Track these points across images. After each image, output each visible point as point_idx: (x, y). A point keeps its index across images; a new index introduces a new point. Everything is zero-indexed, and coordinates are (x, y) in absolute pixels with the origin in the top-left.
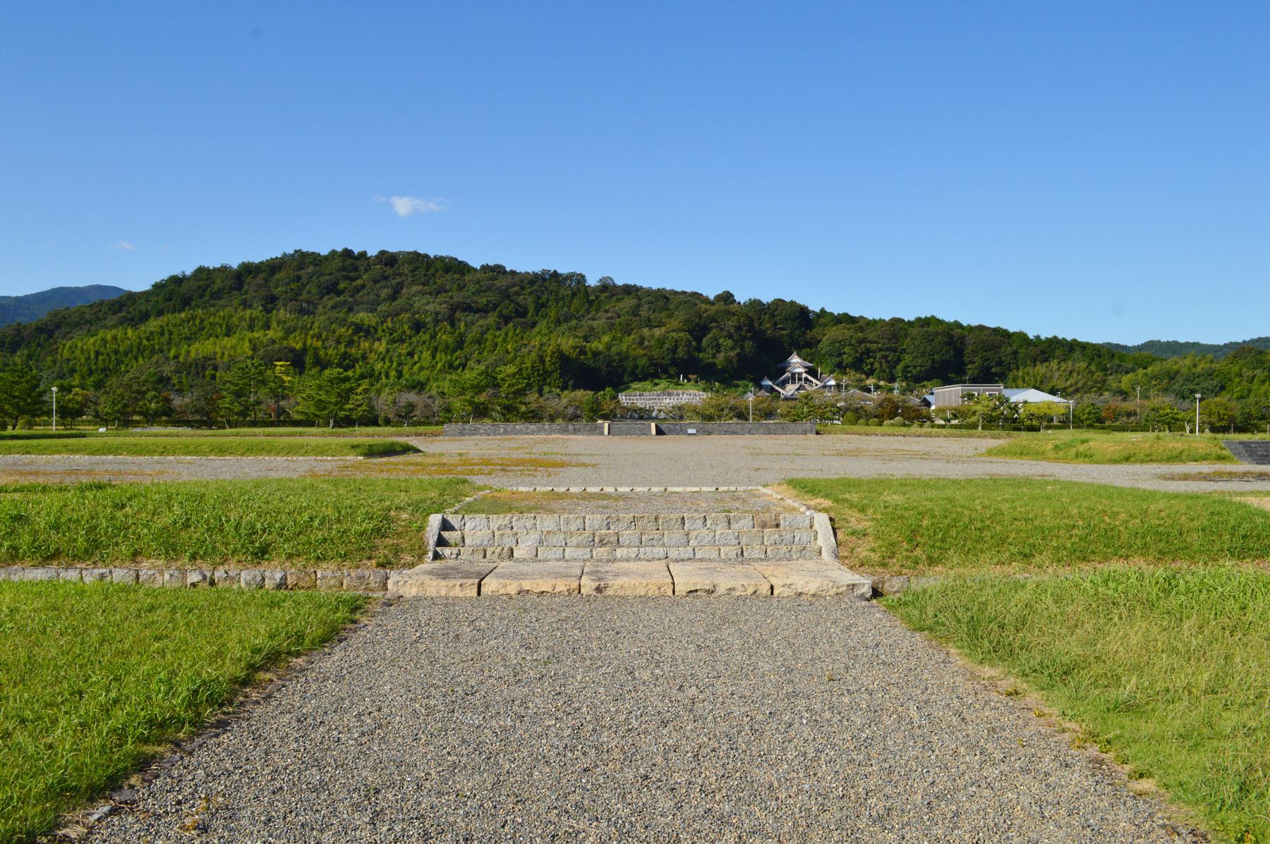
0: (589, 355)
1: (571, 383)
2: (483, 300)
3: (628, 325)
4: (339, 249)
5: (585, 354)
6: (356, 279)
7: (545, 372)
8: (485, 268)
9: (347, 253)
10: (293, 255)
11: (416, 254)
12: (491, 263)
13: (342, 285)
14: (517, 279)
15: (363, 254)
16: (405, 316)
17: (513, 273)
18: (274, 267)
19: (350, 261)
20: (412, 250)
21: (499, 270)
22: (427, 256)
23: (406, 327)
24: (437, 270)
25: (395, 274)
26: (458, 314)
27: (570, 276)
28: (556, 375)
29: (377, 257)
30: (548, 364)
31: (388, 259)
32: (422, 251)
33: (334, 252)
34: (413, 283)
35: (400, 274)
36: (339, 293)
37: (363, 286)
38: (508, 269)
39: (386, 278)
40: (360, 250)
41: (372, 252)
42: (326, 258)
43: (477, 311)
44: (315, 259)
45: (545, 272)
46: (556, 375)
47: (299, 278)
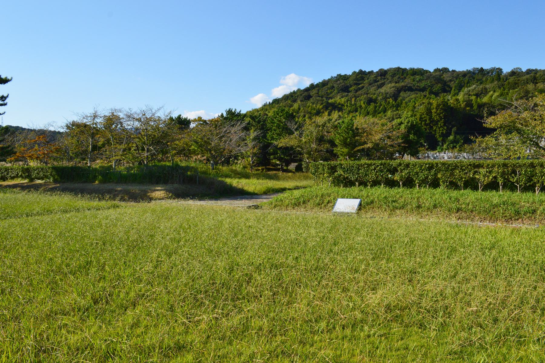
0: (475, 107)
1: (454, 129)
2: (422, 85)
3: (516, 84)
4: (357, 71)
5: (471, 106)
6: (359, 84)
7: (432, 120)
8: (436, 70)
9: (361, 72)
10: (336, 77)
11: (399, 69)
12: (440, 67)
13: (351, 89)
14: (455, 75)
15: (371, 72)
16: (362, 97)
17: (454, 71)
18: (324, 84)
19: (361, 75)
20: (397, 67)
21: (445, 70)
22: (405, 69)
23: (362, 102)
24: (407, 75)
25: (381, 79)
26: (402, 94)
27: (493, 70)
28: (441, 124)
29: (377, 72)
30: (434, 114)
31: (383, 73)
32: (403, 67)
33: (354, 72)
34: (390, 82)
35: (385, 79)
36: (349, 92)
37: (363, 87)
38: (450, 70)
39: (376, 81)
40: (370, 70)
41: (376, 70)
42: (350, 76)
43: (416, 90)
44: (345, 78)
45: (474, 69)
46: (441, 124)
47: (333, 87)
